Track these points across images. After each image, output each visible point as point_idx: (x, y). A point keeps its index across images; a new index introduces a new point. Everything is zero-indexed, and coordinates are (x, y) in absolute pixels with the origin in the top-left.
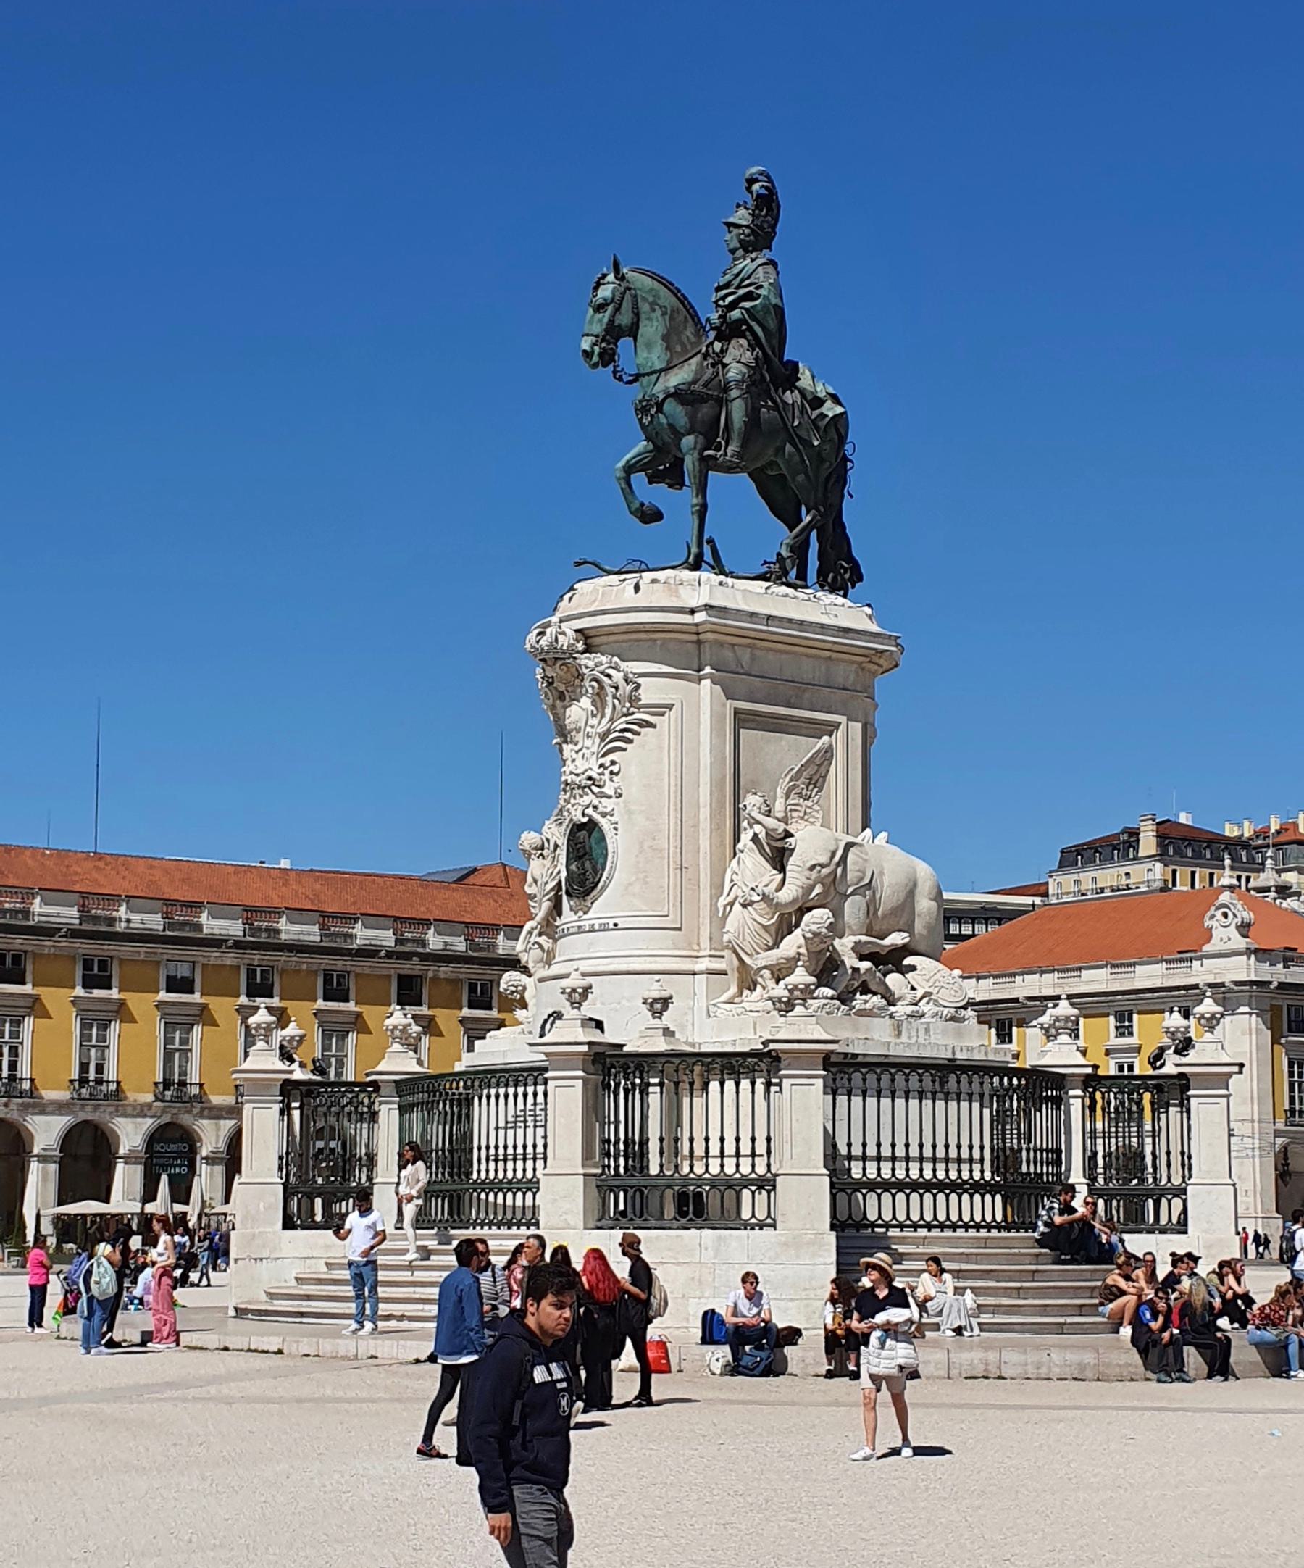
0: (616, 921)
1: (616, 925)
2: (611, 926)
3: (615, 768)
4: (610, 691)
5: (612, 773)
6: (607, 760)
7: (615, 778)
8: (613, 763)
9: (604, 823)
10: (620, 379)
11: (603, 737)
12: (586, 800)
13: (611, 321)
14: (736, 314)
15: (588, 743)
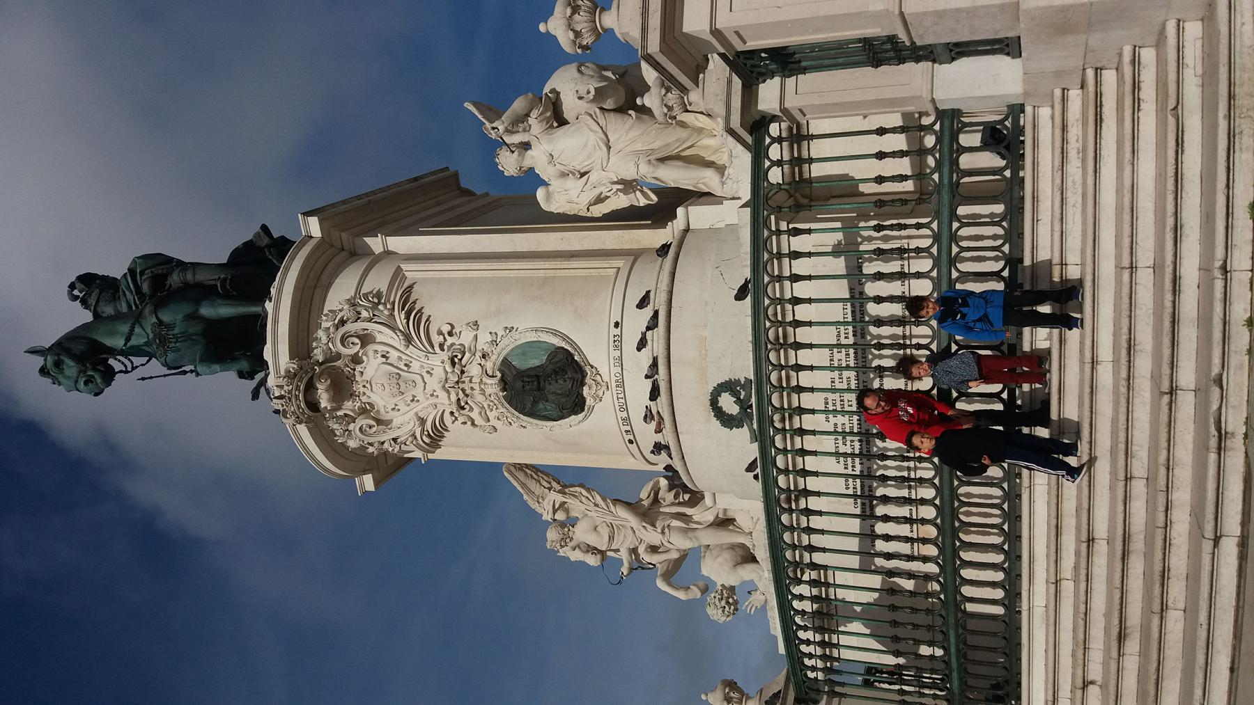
0: (612, 324)
1: (617, 325)
2: (617, 331)
3: (446, 329)
4: (359, 326)
5: (450, 334)
6: (437, 339)
7: (456, 330)
8: (440, 333)
9: (507, 345)
10: (133, 368)
11: (408, 340)
12: (474, 370)
13: (74, 357)
14: (145, 287)
15: (415, 366)
